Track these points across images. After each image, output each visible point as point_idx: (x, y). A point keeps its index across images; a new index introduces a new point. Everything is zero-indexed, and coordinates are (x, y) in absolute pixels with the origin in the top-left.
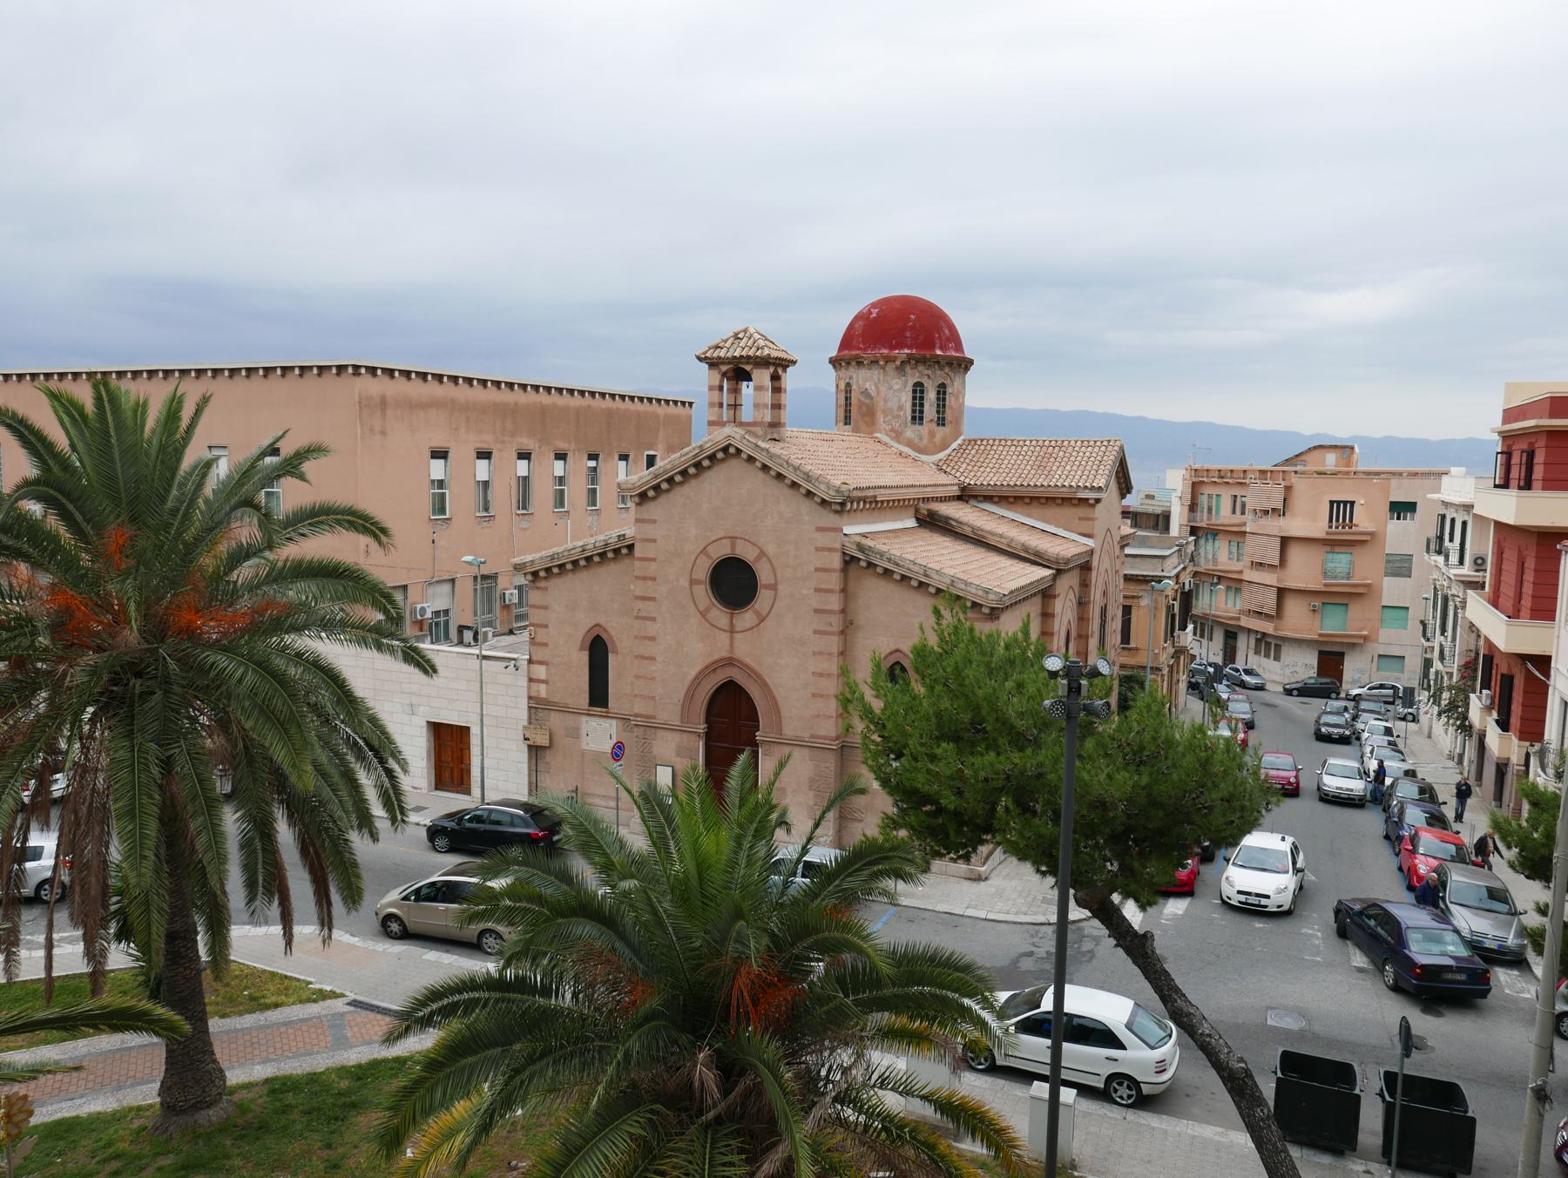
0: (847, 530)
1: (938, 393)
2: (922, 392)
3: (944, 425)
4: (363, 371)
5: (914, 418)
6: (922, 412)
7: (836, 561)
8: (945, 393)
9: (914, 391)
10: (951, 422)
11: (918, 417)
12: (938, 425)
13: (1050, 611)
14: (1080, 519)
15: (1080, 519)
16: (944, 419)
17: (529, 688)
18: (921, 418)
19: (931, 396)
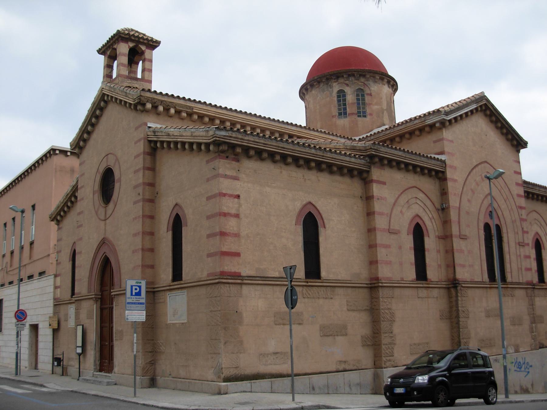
0: (149, 125)
1: (358, 95)
2: (344, 96)
3: (365, 116)
4: (57, 152)
5: (340, 114)
6: (345, 109)
7: (141, 147)
8: (363, 95)
9: (339, 97)
10: (371, 114)
11: (343, 113)
12: (359, 116)
13: (371, 194)
14: (435, 142)
15: (435, 142)
16: (364, 112)
17: (54, 292)
18: (345, 113)
19: (350, 98)
